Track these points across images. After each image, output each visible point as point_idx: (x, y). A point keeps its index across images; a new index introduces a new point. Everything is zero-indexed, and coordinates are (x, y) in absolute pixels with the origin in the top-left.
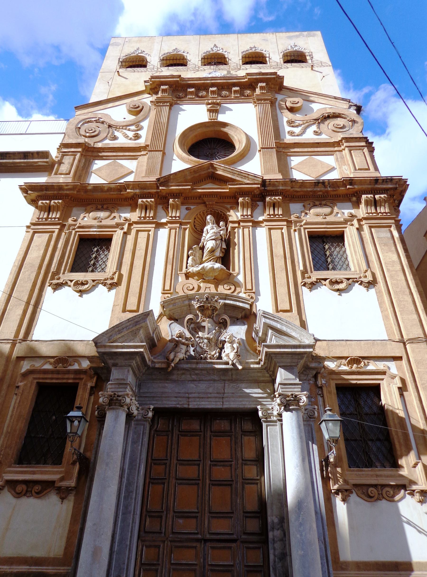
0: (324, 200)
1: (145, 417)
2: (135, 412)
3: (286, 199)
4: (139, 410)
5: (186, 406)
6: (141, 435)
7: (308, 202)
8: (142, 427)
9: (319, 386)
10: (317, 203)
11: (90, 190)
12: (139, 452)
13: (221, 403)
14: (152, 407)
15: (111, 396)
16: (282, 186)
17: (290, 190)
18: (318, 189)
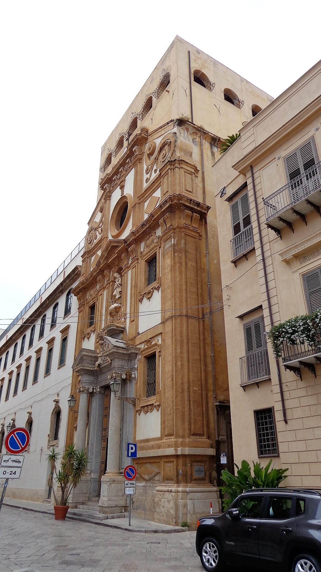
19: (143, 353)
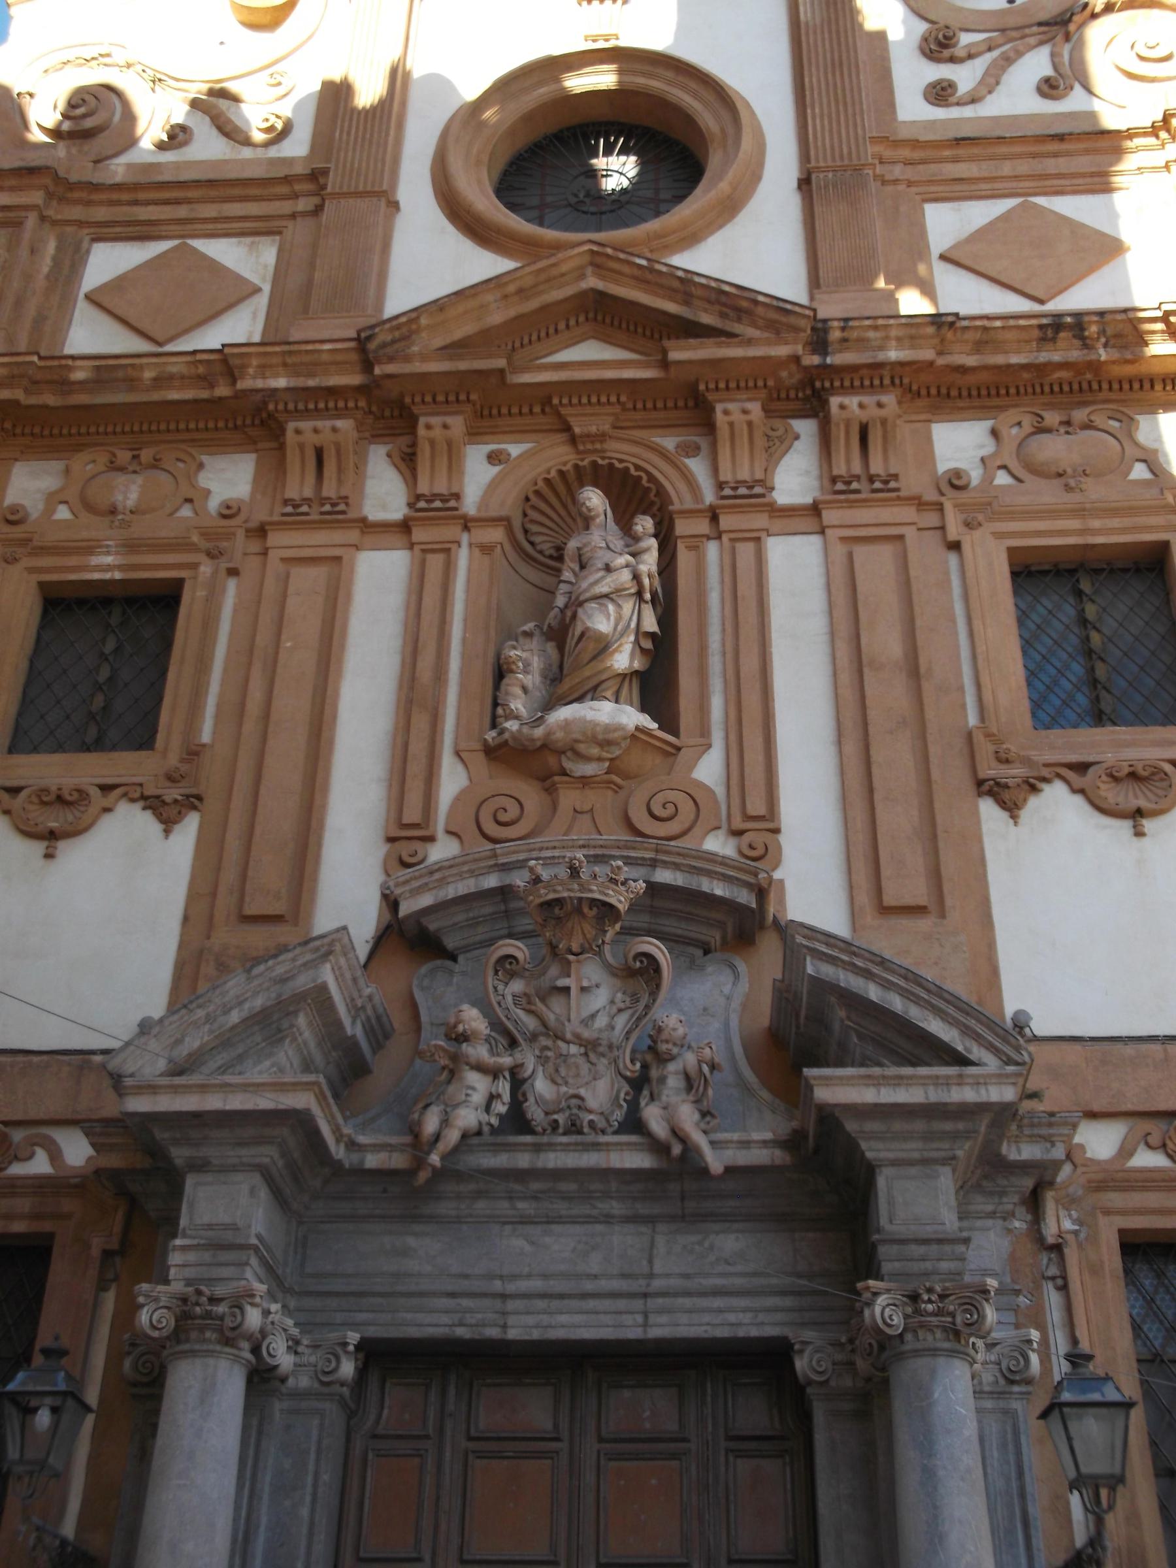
0: (1085, 404)
1: (325, 1378)
2: (284, 1360)
3: (921, 403)
4: (300, 1349)
5: (493, 1333)
6: (313, 1456)
7: (1012, 415)
8: (316, 1422)
9: (1051, 1240)
10: (1052, 418)
11: (80, 382)
12: (305, 1530)
13: (640, 1319)
14: (353, 1337)
15: (184, 1300)
16: (900, 347)
17: (931, 364)
18: (1056, 357)
19: (1115, 1199)
